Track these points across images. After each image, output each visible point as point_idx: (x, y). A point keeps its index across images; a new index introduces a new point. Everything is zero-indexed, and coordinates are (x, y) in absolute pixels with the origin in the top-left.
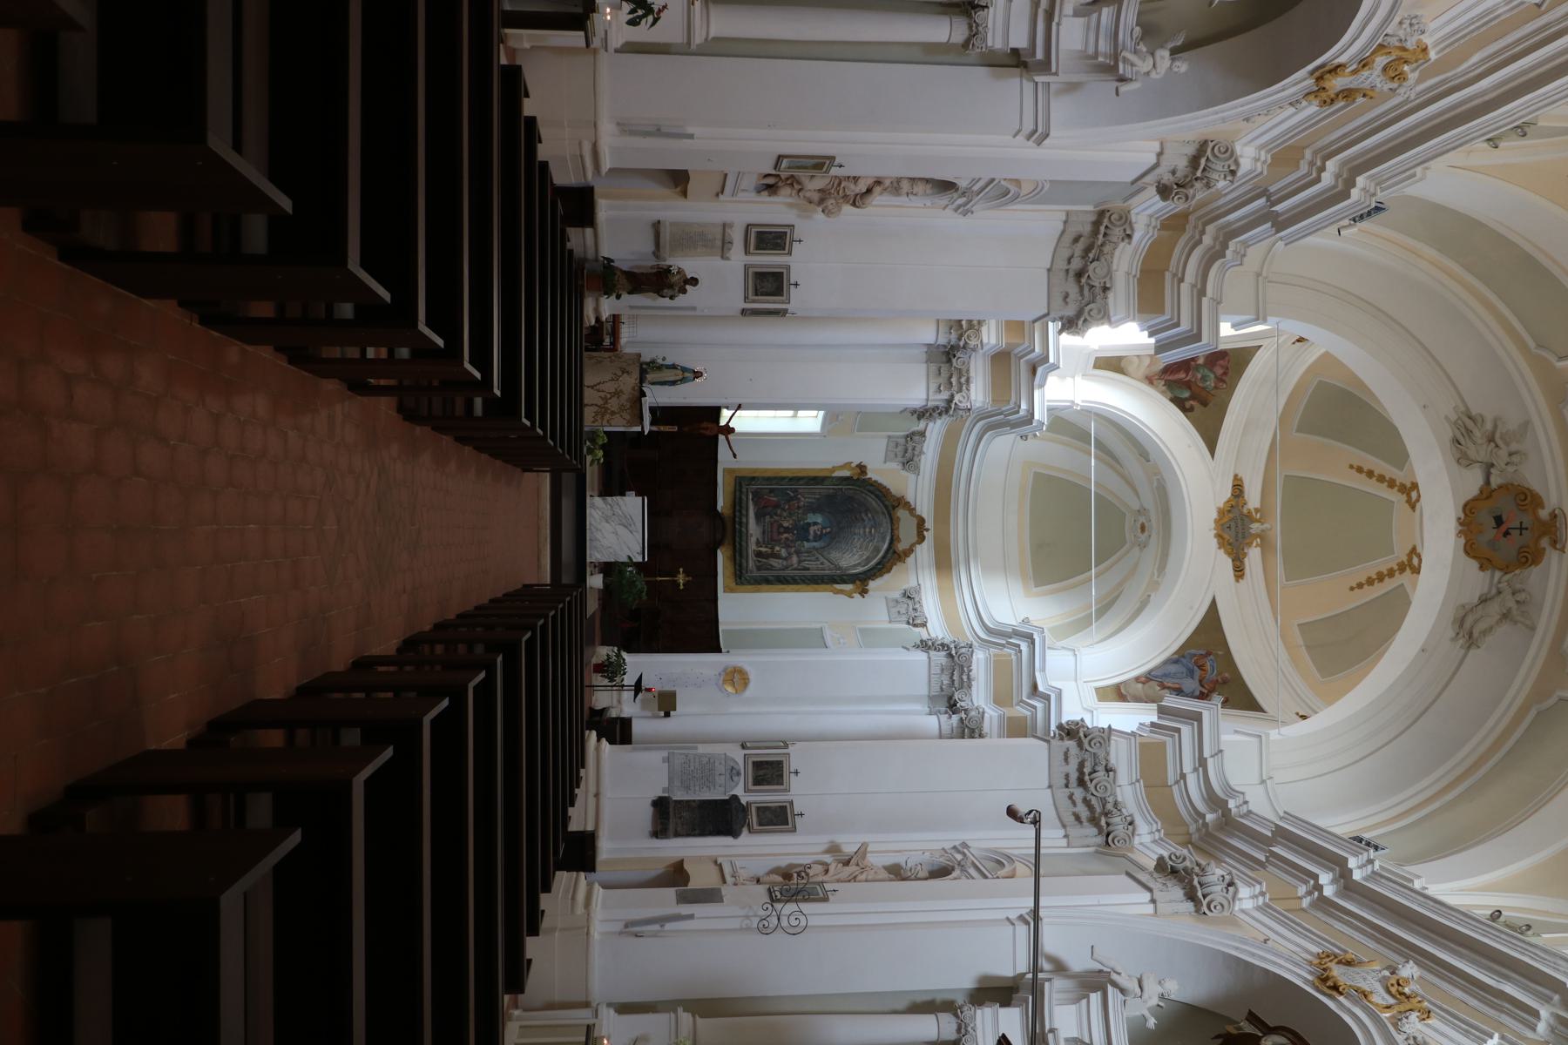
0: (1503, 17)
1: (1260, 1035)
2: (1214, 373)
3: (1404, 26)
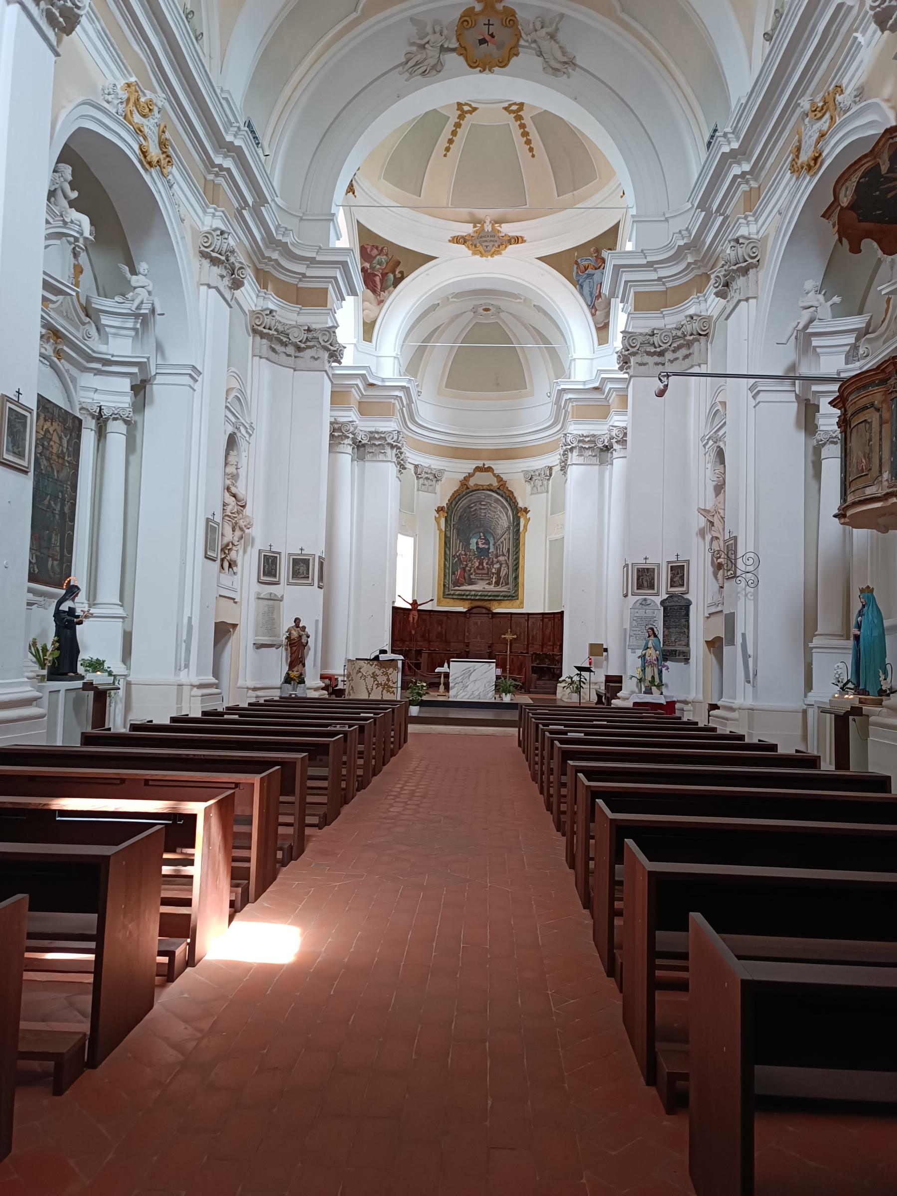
0: (104, 25)
1: (839, 207)
2: (376, 256)
3: (110, 100)
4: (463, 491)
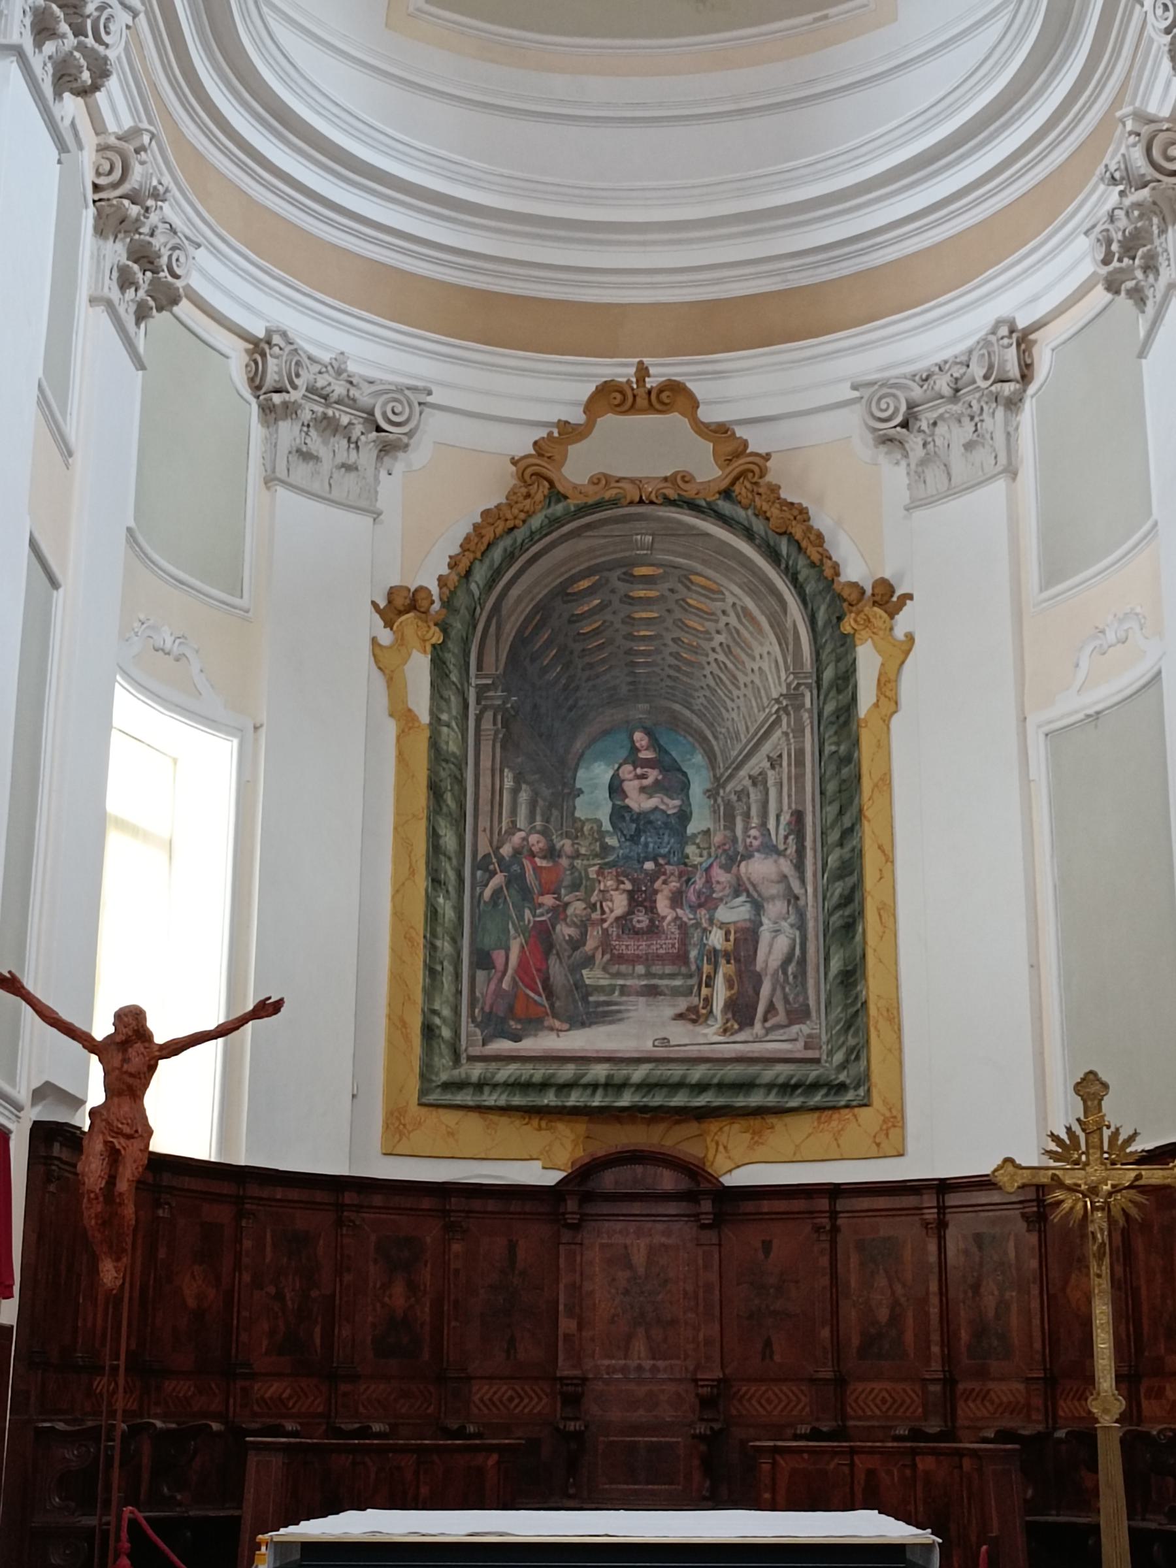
4: (530, 514)
